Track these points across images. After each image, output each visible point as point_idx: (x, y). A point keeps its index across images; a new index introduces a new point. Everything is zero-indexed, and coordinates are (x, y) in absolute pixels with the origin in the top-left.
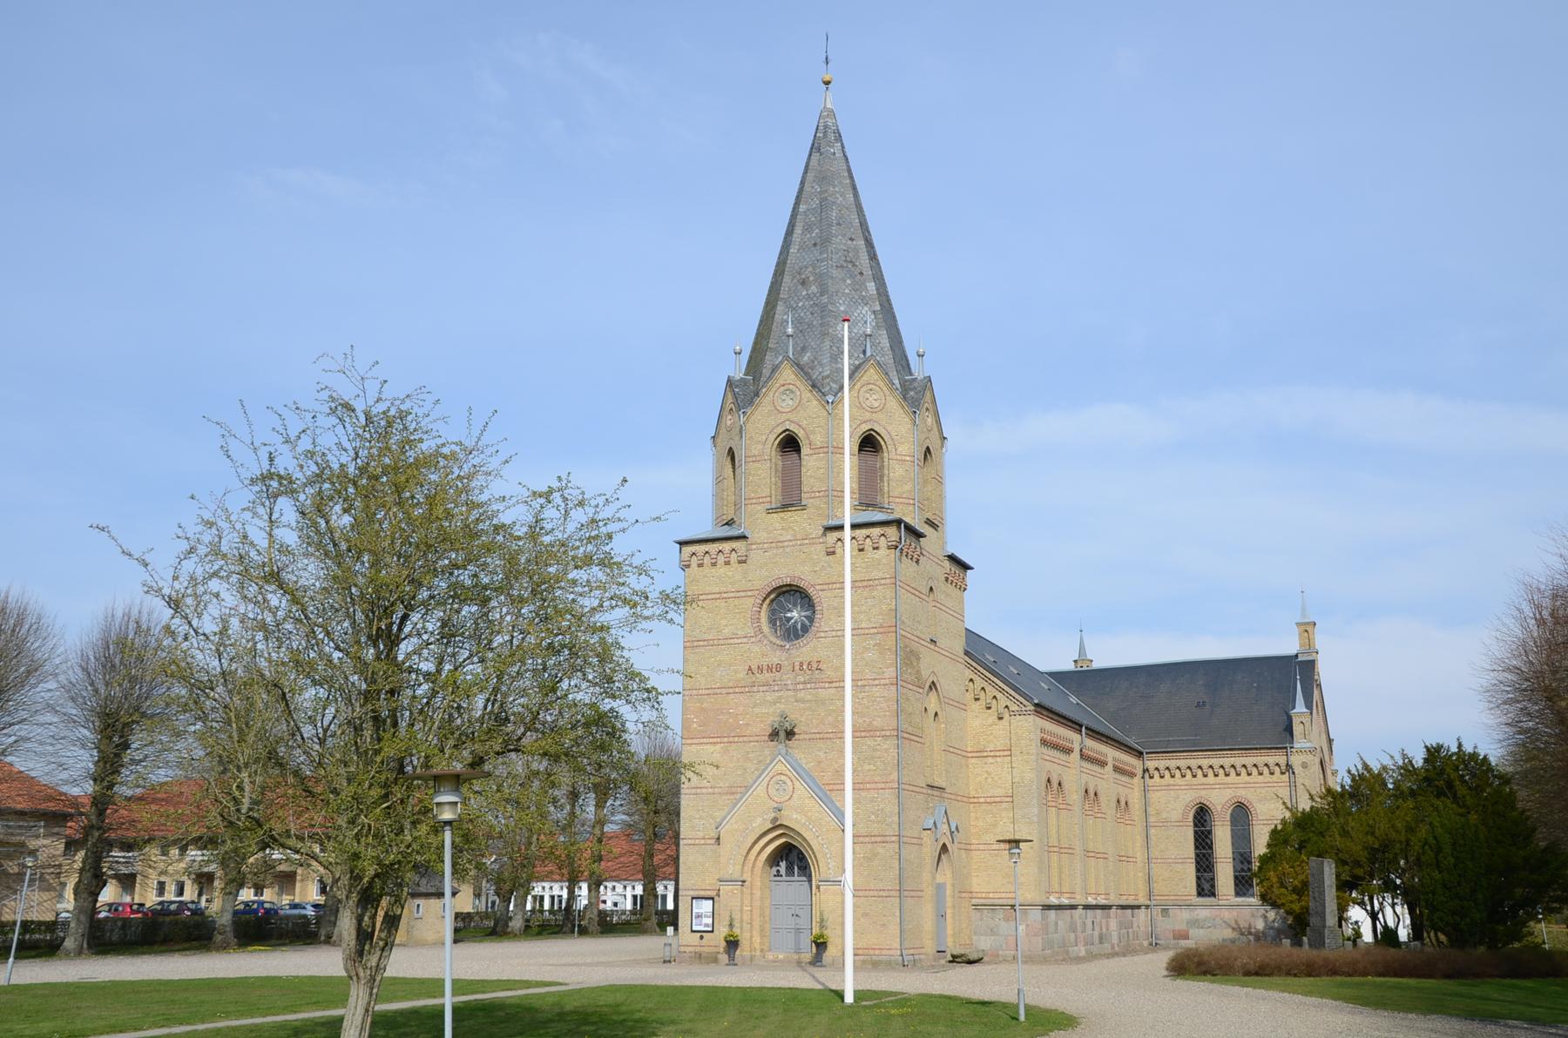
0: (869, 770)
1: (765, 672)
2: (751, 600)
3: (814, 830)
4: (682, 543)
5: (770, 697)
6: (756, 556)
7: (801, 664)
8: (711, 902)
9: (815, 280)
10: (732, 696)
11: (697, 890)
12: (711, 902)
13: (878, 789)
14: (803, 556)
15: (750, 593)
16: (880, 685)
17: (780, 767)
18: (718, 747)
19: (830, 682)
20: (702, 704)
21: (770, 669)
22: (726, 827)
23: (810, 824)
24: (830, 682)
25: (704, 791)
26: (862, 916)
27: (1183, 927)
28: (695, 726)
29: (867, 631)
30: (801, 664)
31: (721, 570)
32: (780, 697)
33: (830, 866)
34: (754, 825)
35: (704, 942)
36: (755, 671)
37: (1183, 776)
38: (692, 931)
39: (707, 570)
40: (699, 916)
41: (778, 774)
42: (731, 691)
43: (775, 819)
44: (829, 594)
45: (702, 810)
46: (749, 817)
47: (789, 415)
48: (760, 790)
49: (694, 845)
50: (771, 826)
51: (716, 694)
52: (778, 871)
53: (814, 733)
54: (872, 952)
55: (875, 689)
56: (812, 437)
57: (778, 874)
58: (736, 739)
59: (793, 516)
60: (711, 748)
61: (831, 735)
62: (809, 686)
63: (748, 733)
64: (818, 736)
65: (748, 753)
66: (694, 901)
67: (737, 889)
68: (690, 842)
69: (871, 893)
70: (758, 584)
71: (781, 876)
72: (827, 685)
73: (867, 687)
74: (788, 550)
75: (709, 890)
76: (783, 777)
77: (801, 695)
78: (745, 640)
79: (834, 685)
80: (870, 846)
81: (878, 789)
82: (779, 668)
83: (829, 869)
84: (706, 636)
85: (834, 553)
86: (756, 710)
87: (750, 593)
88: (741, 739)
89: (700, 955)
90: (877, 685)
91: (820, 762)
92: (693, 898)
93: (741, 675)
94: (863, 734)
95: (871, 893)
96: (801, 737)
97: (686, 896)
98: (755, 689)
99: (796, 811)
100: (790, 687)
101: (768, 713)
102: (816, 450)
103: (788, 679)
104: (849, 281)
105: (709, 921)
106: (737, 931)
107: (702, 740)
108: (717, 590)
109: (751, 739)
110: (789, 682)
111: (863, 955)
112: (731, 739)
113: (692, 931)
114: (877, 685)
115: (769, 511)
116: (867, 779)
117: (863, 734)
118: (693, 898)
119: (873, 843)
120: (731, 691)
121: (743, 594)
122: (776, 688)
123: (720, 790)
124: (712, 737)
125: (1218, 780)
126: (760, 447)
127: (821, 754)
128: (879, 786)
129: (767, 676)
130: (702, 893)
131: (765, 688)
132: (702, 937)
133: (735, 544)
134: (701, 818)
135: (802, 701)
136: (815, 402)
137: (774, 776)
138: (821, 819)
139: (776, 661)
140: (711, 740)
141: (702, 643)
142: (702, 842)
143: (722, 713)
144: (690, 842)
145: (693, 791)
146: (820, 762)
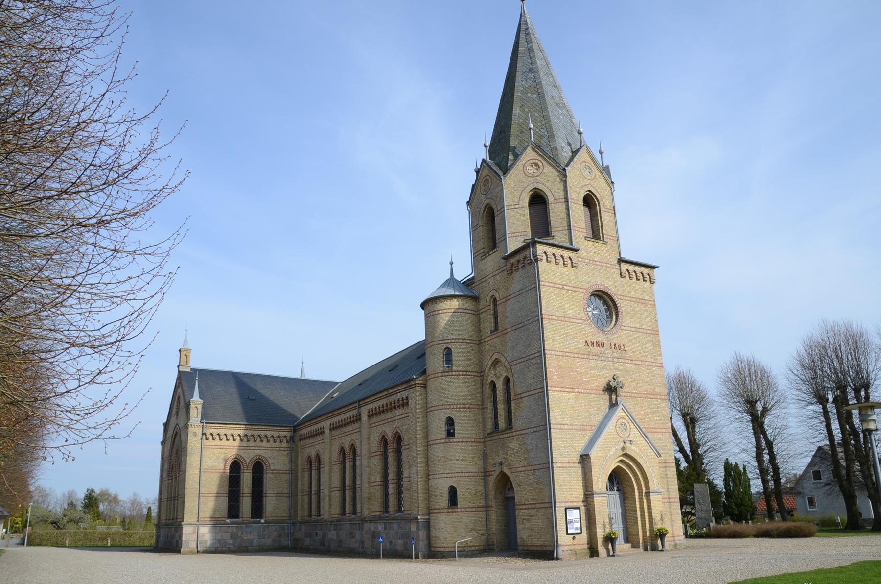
1: (595, 346)
5: (600, 364)
8: (578, 510)
10: (577, 360)
11: (567, 502)
12: (578, 510)
14: (608, 274)
15: (581, 290)
18: (572, 395)
21: (598, 344)
25: (566, 427)
28: (556, 378)
29: (646, 331)
32: (605, 365)
34: (611, 453)
35: (576, 541)
36: (590, 345)
37: (255, 441)
41: (622, 418)
42: (576, 356)
45: (566, 441)
49: (562, 467)
58: (583, 391)
60: (567, 395)
63: (589, 387)
67: (604, 500)
70: (585, 285)
72: (630, 362)
74: (599, 267)
75: (575, 502)
76: (624, 421)
77: (617, 365)
78: (581, 322)
82: (603, 345)
84: (557, 314)
87: (581, 290)
88: (585, 391)
93: (582, 345)
97: (561, 507)
98: (590, 357)
100: (610, 359)
103: (609, 353)
105: (578, 525)
107: (561, 389)
108: (560, 282)
109: (592, 392)
110: (609, 356)
112: (580, 391)
120: (576, 356)
121: (576, 289)
122: (603, 359)
123: (576, 427)
124: (568, 388)
125: (214, 443)
129: (596, 349)
130: (571, 505)
131: (596, 358)
132: (574, 538)
134: (565, 447)
139: (600, 340)
140: (567, 390)
141: (554, 318)
142: (568, 465)
143: (572, 371)
145: (559, 426)
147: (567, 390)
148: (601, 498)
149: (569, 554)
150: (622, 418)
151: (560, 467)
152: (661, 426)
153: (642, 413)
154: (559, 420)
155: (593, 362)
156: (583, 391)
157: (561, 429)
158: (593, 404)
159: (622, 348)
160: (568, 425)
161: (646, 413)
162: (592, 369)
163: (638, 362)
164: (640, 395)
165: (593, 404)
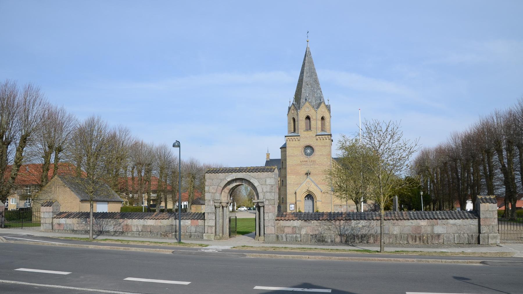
2: (301, 148)
4: (285, 136)
6: (301, 139)
7: (311, 161)
8: (294, 205)
9: (310, 84)
17: (309, 180)
21: (305, 161)
27: (353, 209)
30: (311, 161)
31: (294, 142)
39: (291, 142)
40: (291, 207)
43: (308, 190)
44: (317, 148)
47: (308, 112)
48: (304, 184)
56: (313, 117)
57: (306, 199)
59: (309, 132)
70: (302, 145)
82: (307, 161)
84: (292, 155)
85: (318, 140)
86: (302, 169)
102: (314, 120)
103: (309, 163)
104: (316, 85)
105: (294, 208)
106: (300, 210)
108: (293, 146)
115: (304, 131)
126: (302, 118)
127: (316, 178)
129: (304, 163)
130: (292, 203)
133: (297, 137)
135: (312, 168)
136: (313, 110)
139: (306, 160)
153: (320, 179)
154: (290, 182)
158: (302, 178)
159: (314, 161)
165: (302, 178)
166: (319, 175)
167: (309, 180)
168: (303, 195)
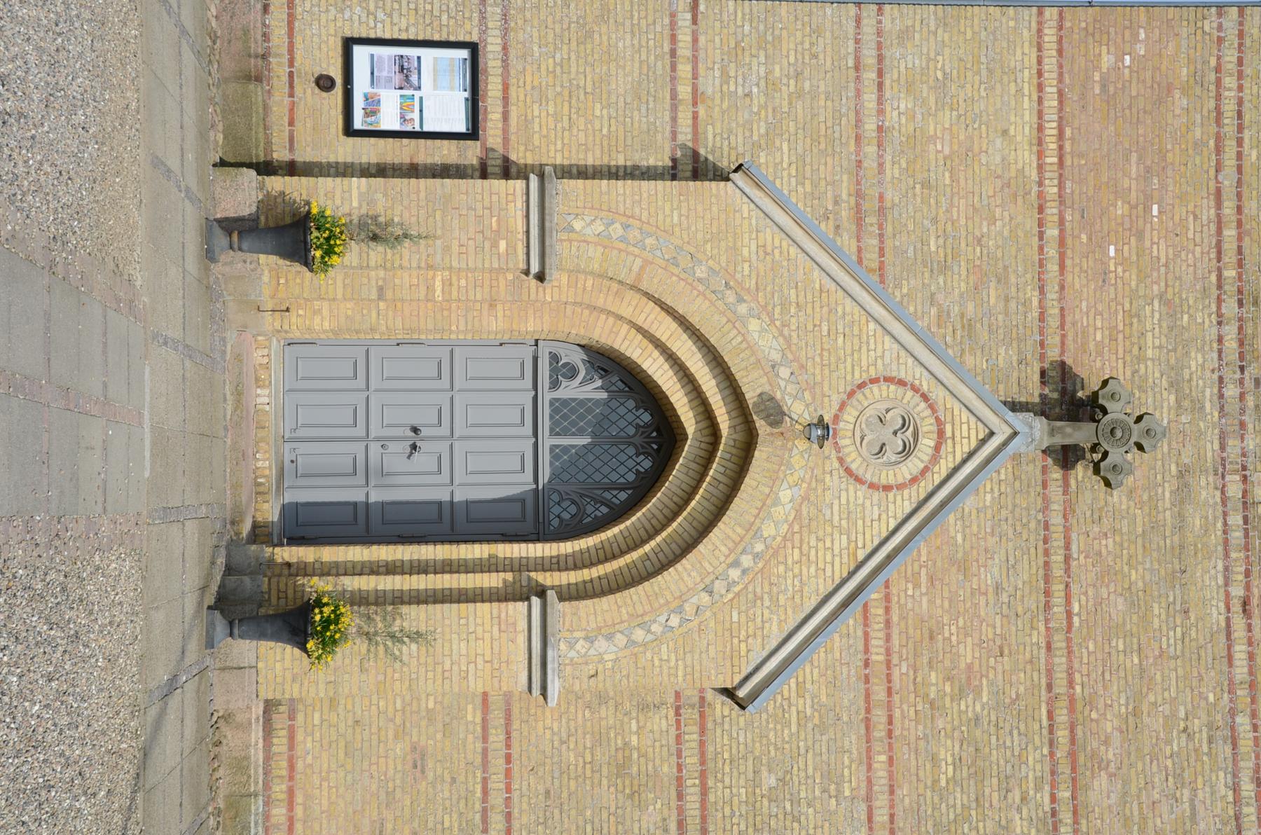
0: (934, 759)
3: (734, 574)
5: (1199, 363)
12: (461, 127)
13: (869, 798)
16: (1237, 801)
18: (1027, 157)
19: (1245, 603)
20: (1185, 91)
22: (746, 208)
23: (757, 556)
24: (1245, 603)
26: (414, 749)
28: (1107, 61)
32: (1197, 407)
33: (602, 644)
34: (754, 325)
35: (307, 92)
38: (348, 44)
40: (406, 74)
41: (941, 433)
43: (776, 415)
45: (800, 94)
46: (784, 305)
49: (673, 53)
50: (750, 396)
51: (1219, 150)
52: (572, 372)
53: (1067, 547)
54: (279, 789)
55: (1222, 779)
57: (566, 372)
58: (1052, 232)
61: (1058, 610)
62: (1236, 519)
63: (1075, 280)
64: (1057, 558)
65: (1002, 280)
66: (464, 54)
68: (684, 38)
69: (497, 783)
71: (555, 384)
72: (1237, 591)
73: (1228, 749)
75: (505, 117)
76: (927, 443)
77: (1205, 488)
79: (1239, 622)
80: (668, 769)
81: (869, 798)
83: (590, 640)
86: (1153, 314)
88: (1052, 252)
89: (258, 79)
90: (1236, 789)
91: (964, 567)
92: (473, 48)
94: (1062, 735)
95: (497, 783)
96: (1055, 490)
98: (1230, 308)
99: (806, 498)
100: (1233, 444)
101: (1141, 359)
105: (389, 120)
106: (352, 254)
107: (1051, 90)
109: (1052, 294)
111: (268, 758)
112: (1052, 210)
113: (348, 44)
114: (1236, 789)
116: (902, 753)
117: (1062, 735)
118: (473, 48)
119: (679, 780)
122: (1231, 391)
123: (870, 164)
127: (990, 575)
128: (881, 801)
131: (1231, 344)
132: (324, 83)
134: (771, 85)
137: (932, 407)
138: (775, 601)
140: (1051, 128)
142: (684, 91)
144: (684, 38)
145: (869, 57)
146: (964, 567)
147: (1051, 128)
148: (520, 226)
149: (246, 32)
150: (941, 433)
151: (673, 39)
152: (903, 791)
153: (968, 654)
155: (1206, 318)
156: (1052, 232)
157: (857, 68)
158: (993, 294)
160: (881, 112)
161: (966, 686)
162: (1172, 308)
163: (1240, 651)
164: (1059, 642)
165: (993, 294)
166: (1038, 637)
167: (965, 434)
168: (667, 330)
